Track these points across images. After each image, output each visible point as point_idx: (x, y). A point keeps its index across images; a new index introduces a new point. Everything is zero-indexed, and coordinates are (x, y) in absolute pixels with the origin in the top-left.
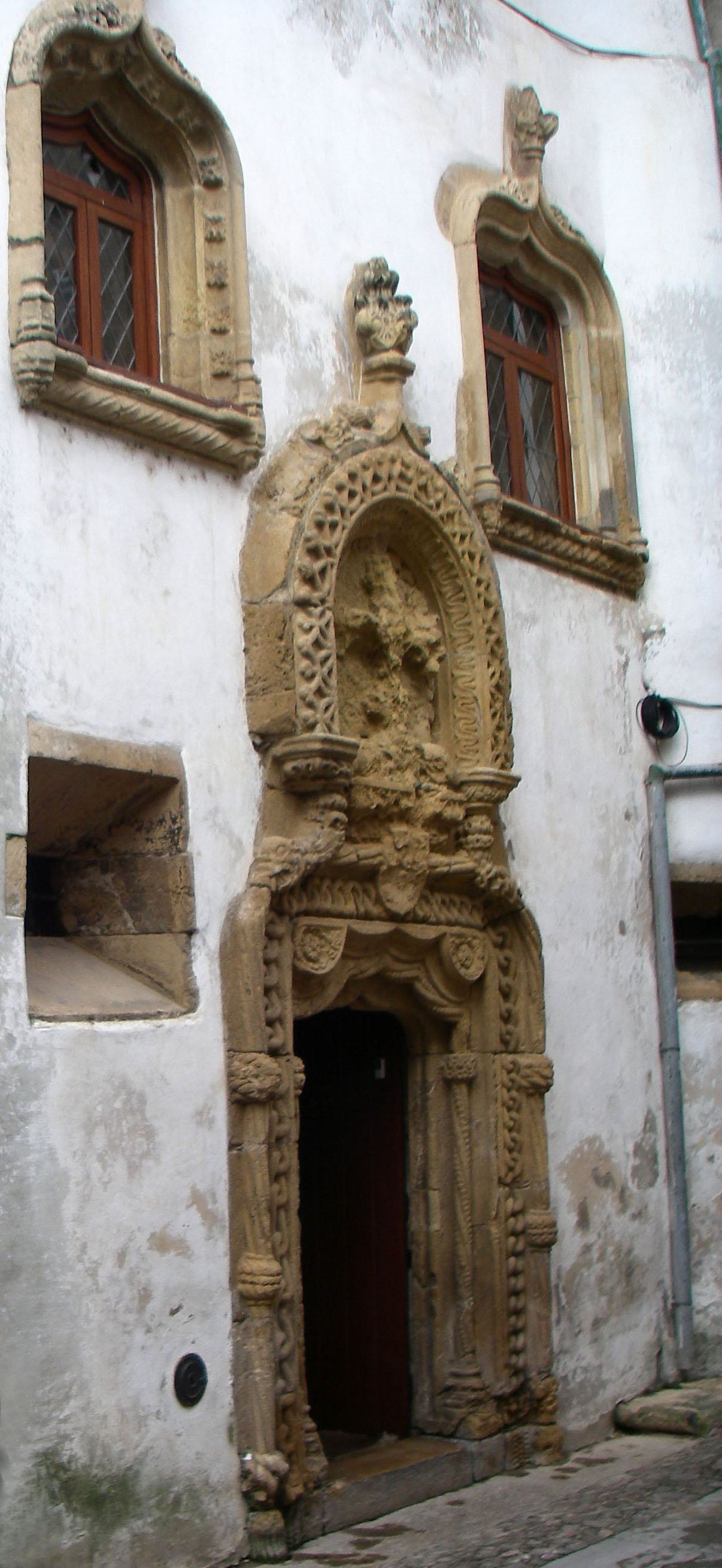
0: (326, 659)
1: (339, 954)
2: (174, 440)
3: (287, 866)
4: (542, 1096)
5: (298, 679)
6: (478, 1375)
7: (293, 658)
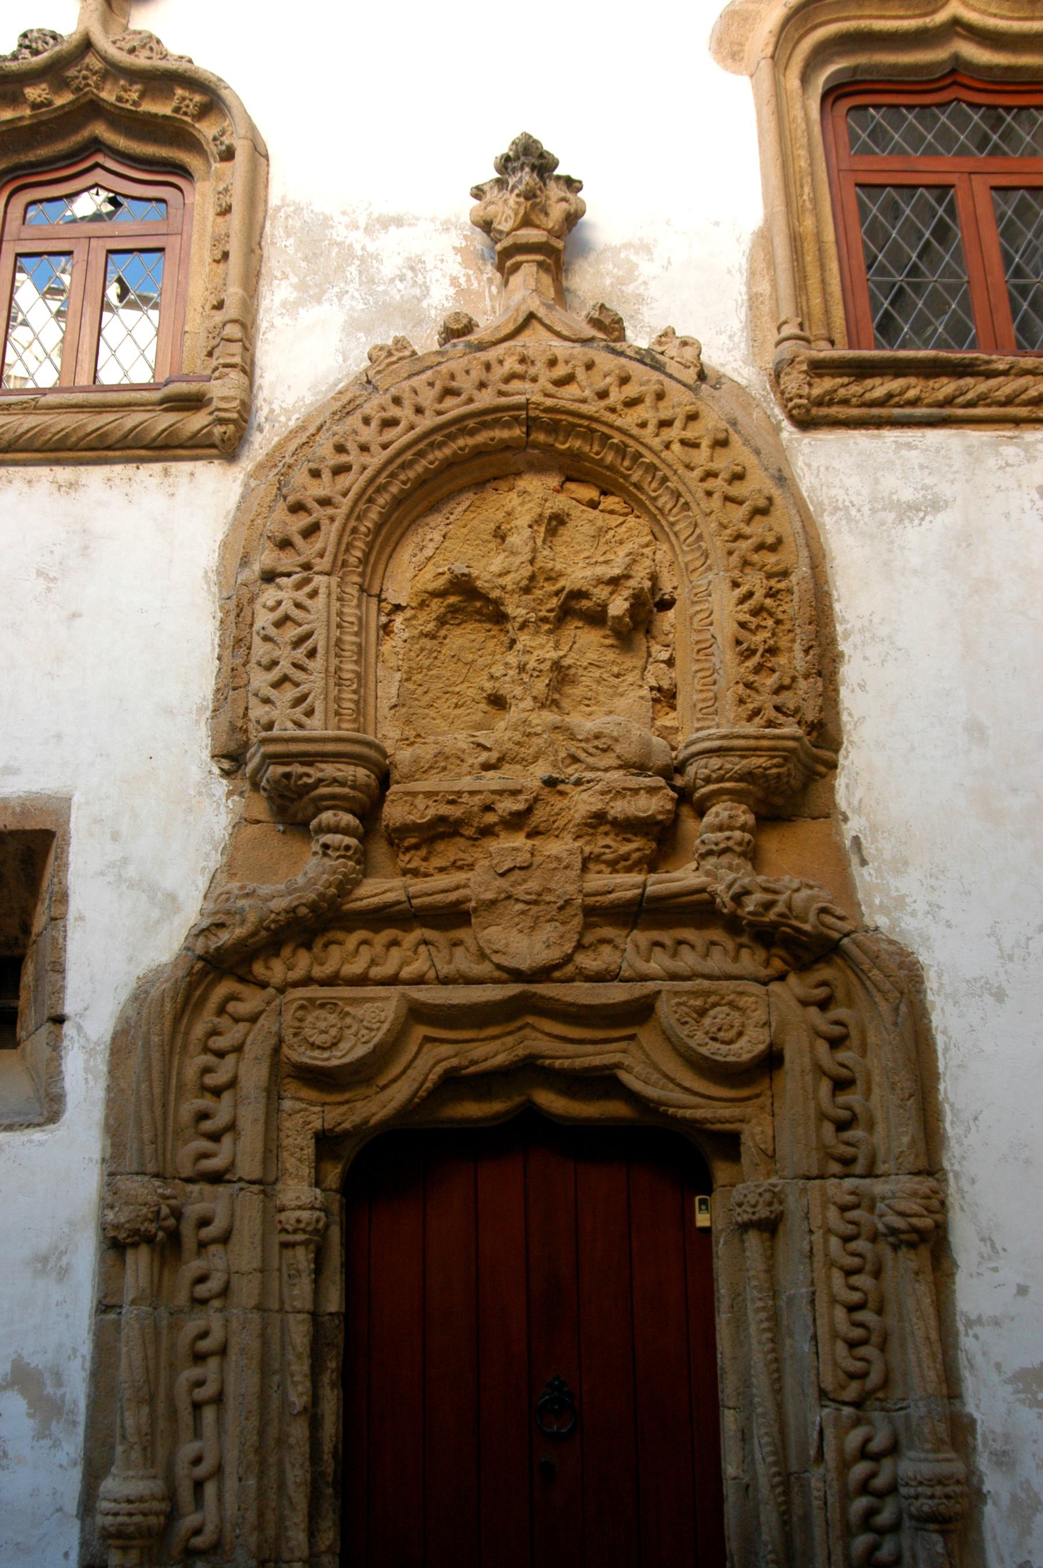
3: (219, 918)
7: (249, 648)
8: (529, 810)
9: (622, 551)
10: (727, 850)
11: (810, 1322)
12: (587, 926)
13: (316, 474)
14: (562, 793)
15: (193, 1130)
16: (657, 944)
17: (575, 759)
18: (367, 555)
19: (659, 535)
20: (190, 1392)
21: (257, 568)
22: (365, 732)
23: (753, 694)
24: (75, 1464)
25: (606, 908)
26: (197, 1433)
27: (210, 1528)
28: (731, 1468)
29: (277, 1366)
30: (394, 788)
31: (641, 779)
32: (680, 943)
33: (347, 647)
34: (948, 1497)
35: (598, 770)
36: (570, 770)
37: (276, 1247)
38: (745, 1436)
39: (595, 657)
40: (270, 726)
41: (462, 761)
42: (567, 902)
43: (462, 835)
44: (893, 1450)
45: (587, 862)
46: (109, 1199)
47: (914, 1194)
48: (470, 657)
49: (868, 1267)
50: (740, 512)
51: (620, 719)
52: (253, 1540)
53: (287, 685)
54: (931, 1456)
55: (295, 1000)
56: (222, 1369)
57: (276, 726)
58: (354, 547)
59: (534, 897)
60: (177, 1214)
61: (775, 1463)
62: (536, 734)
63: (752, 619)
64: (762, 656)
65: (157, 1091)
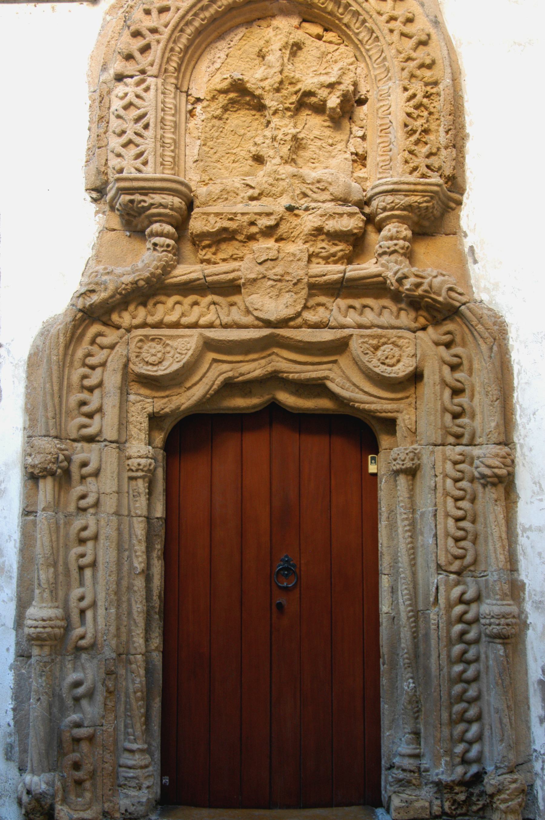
3: (91, 287)
7: (108, 123)
8: (277, 225)
9: (336, 67)
10: (395, 252)
11: (433, 527)
12: (310, 295)
13: (148, 12)
14: (296, 215)
15: (76, 412)
16: (351, 307)
17: (305, 195)
18: (180, 66)
19: (359, 57)
20: (77, 560)
21: (112, 72)
22: (178, 176)
23: (413, 157)
24: (12, 600)
25: (322, 285)
26: (82, 584)
27: (89, 635)
28: (385, 607)
29: (126, 547)
30: (196, 210)
31: (345, 208)
32: (365, 306)
33: (167, 123)
34: (508, 625)
35: (319, 201)
36: (302, 202)
37: (126, 480)
38: (393, 590)
39: (319, 133)
40: (121, 171)
41: (237, 195)
42: (299, 281)
43: (237, 240)
44: (478, 599)
45: (310, 257)
46: (29, 451)
47: (497, 455)
48: (242, 132)
49: (468, 497)
50: (412, 43)
51: (332, 171)
52: (114, 642)
53: (131, 146)
54: (499, 602)
55: (137, 336)
56: (95, 548)
57: (125, 171)
58: (172, 60)
59: (279, 277)
60: (68, 459)
61: (410, 605)
62: (282, 179)
63: (415, 111)
64: (420, 134)
65: (56, 388)
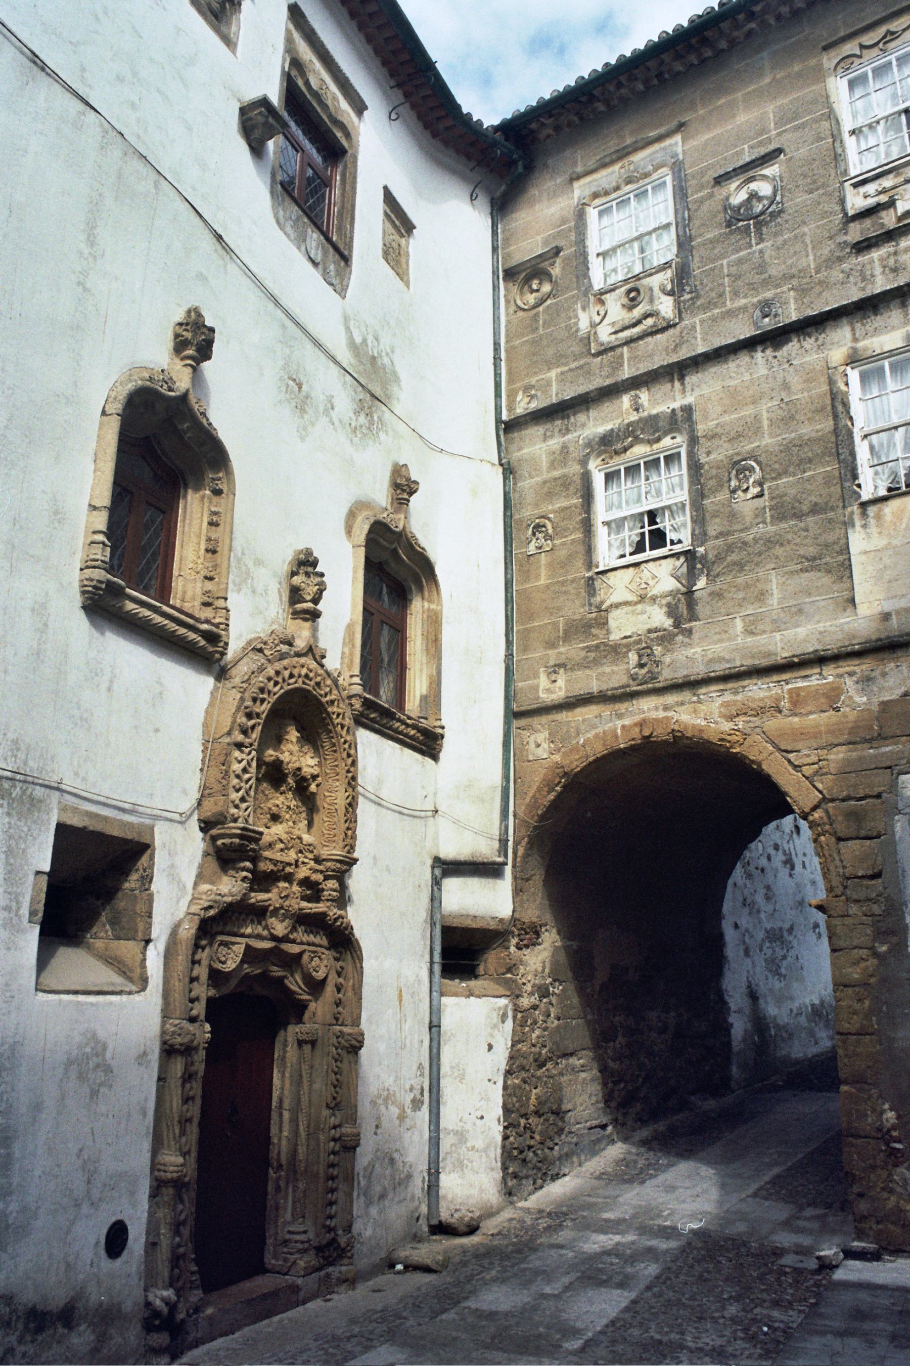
0: (249, 779)
1: (238, 960)
2: (173, 639)
4: (356, 1053)
5: (231, 790)
6: (305, 1232)
